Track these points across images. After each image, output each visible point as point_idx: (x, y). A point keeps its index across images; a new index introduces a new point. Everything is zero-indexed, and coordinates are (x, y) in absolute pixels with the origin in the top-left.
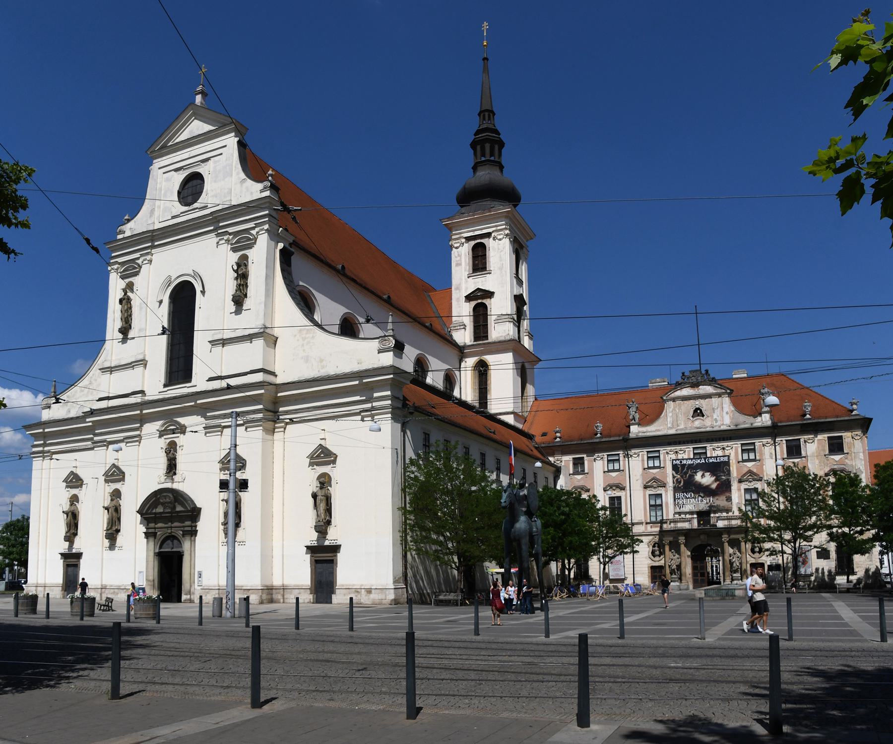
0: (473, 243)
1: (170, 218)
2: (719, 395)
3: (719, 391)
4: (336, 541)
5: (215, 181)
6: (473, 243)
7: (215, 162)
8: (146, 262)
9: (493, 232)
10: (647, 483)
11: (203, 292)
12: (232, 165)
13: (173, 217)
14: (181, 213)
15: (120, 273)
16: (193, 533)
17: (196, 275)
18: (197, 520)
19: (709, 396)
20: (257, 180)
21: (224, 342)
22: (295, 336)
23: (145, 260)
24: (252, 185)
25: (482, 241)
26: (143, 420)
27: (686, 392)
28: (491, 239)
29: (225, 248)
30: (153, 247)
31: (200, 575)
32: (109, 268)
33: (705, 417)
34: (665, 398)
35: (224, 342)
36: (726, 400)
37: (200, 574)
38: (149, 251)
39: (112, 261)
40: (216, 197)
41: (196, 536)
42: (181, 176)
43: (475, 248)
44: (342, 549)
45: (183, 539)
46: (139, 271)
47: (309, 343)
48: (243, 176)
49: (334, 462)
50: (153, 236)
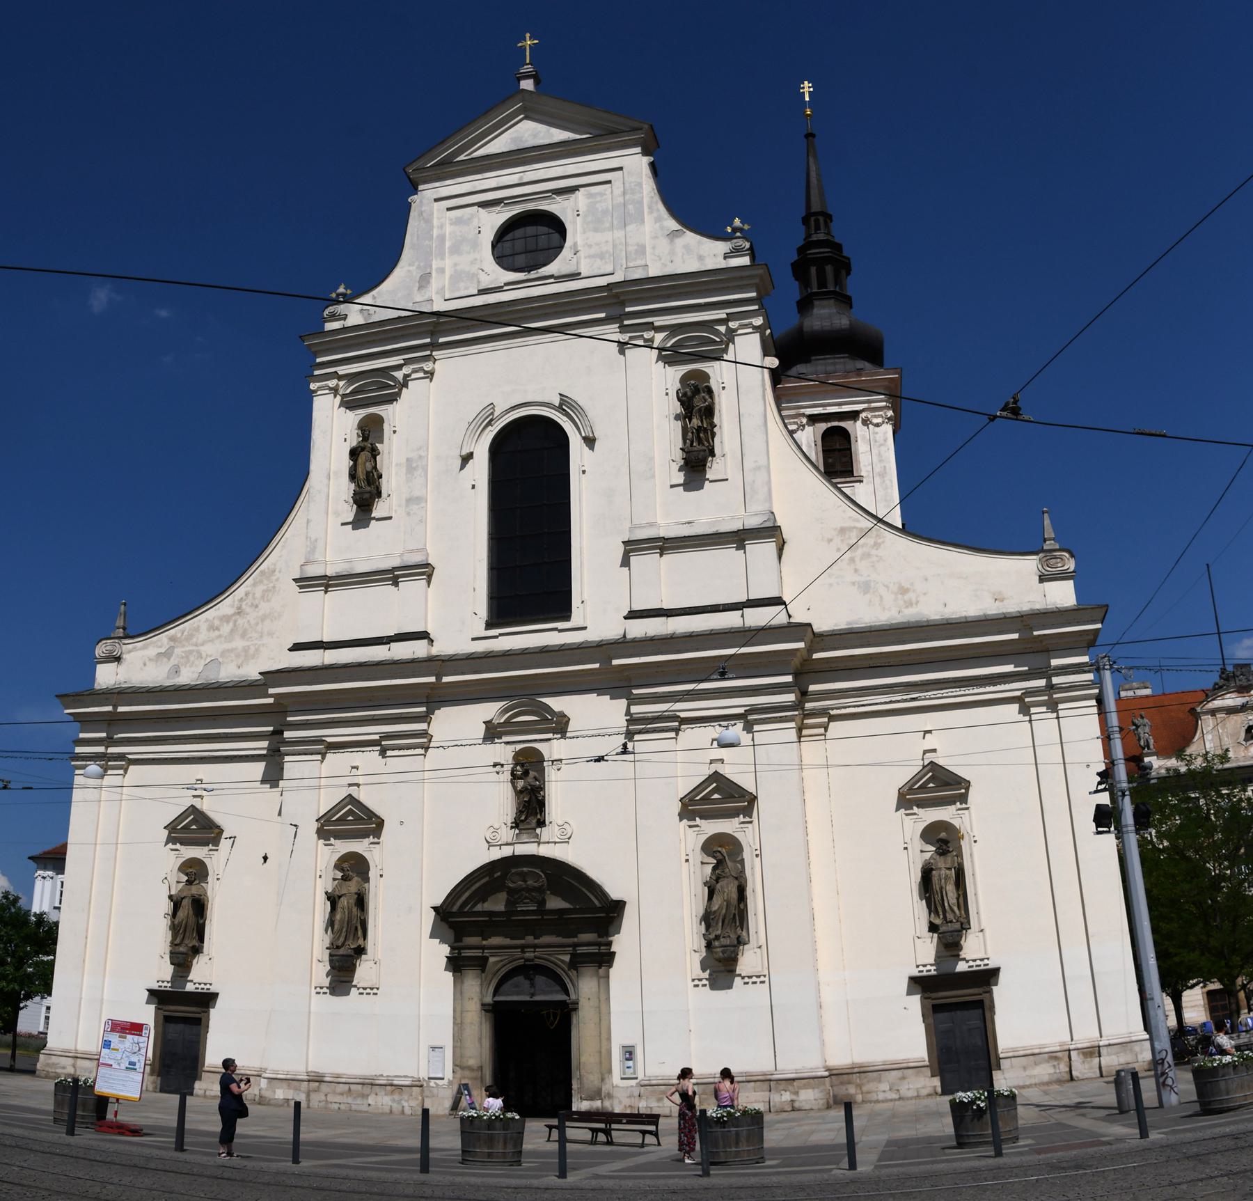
1: (476, 292)
4: (986, 962)
5: (596, 230)
7: (590, 196)
8: (421, 375)
11: (590, 442)
12: (641, 202)
14: (506, 284)
15: (343, 396)
16: (605, 959)
17: (565, 405)
18: (611, 929)
20: (715, 234)
21: (665, 545)
22: (830, 540)
23: (421, 369)
24: (699, 242)
30: (435, 346)
31: (629, 1053)
32: (313, 386)
35: (665, 545)
37: (631, 1053)
38: (428, 353)
39: (316, 373)
40: (601, 259)
41: (611, 966)
44: (1002, 976)
45: (573, 973)
46: (399, 394)
47: (868, 555)
48: (673, 224)
49: (963, 798)
50: (436, 324)
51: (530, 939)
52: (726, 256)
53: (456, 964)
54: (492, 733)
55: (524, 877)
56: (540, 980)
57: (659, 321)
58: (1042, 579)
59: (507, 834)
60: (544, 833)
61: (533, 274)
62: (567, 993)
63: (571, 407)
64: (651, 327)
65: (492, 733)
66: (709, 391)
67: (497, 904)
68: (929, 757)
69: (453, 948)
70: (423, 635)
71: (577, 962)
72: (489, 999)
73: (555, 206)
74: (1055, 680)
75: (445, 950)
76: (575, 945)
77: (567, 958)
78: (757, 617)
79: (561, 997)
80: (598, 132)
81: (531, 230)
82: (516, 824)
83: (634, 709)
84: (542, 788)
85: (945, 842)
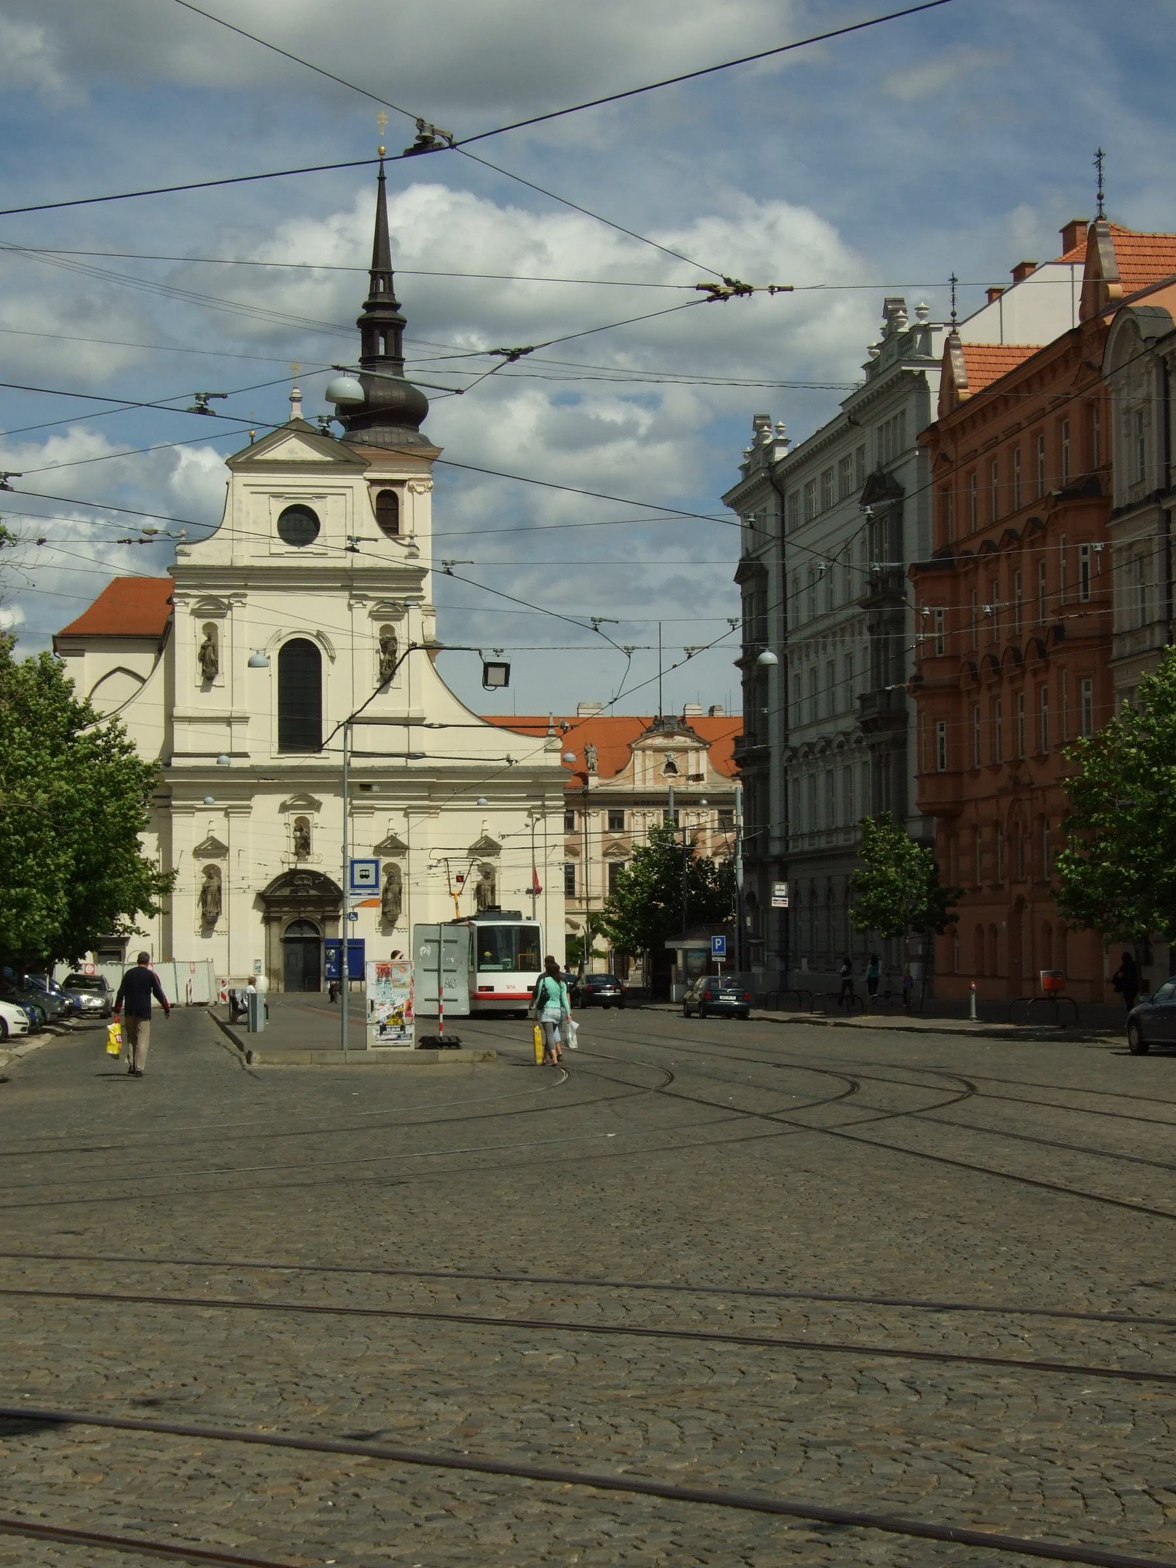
0: (378, 489)
2: (697, 750)
3: (696, 744)
6: (378, 489)
9: (410, 479)
10: (608, 849)
11: (332, 659)
13: (272, 555)
17: (319, 635)
19: (684, 750)
25: (393, 489)
26: (249, 791)
27: (659, 741)
28: (406, 489)
29: (362, 612)
30: (246, 587)
33: (679, 774)
34: (633, 745)
36: (704, 755)
42: (284, 505)
43: (381, 495)
51: (302, 909)
52: (406, 558)
53: (267, 920)
54: (284, 808)
55: (302, 879)
56: (306, 928)
57: (371, 594)
58: (546, 751)
59: (293, 858)
60: (310, 858)
61: (302, 549)
62: (318, 933)
63: (323, 637)
64: (366, 598)
65: (284, 808)
66: (395, 639)
67: (286, 892)
68: (485, 833)
69: (265, 912)
70: (245, 755)
71: (324, 919)
72: (282, 937)
73: (315, 506)
74: (546, 803)
75: (260, 915)
76: (323, 912)
77: (319, 917)
78: (413, 763)
79: (315, 935)
80: (342, 459)
81: (298, 516)
82: (296, 854)
83: (354, 802)
84: (309, 838)
85: (489, 873)
